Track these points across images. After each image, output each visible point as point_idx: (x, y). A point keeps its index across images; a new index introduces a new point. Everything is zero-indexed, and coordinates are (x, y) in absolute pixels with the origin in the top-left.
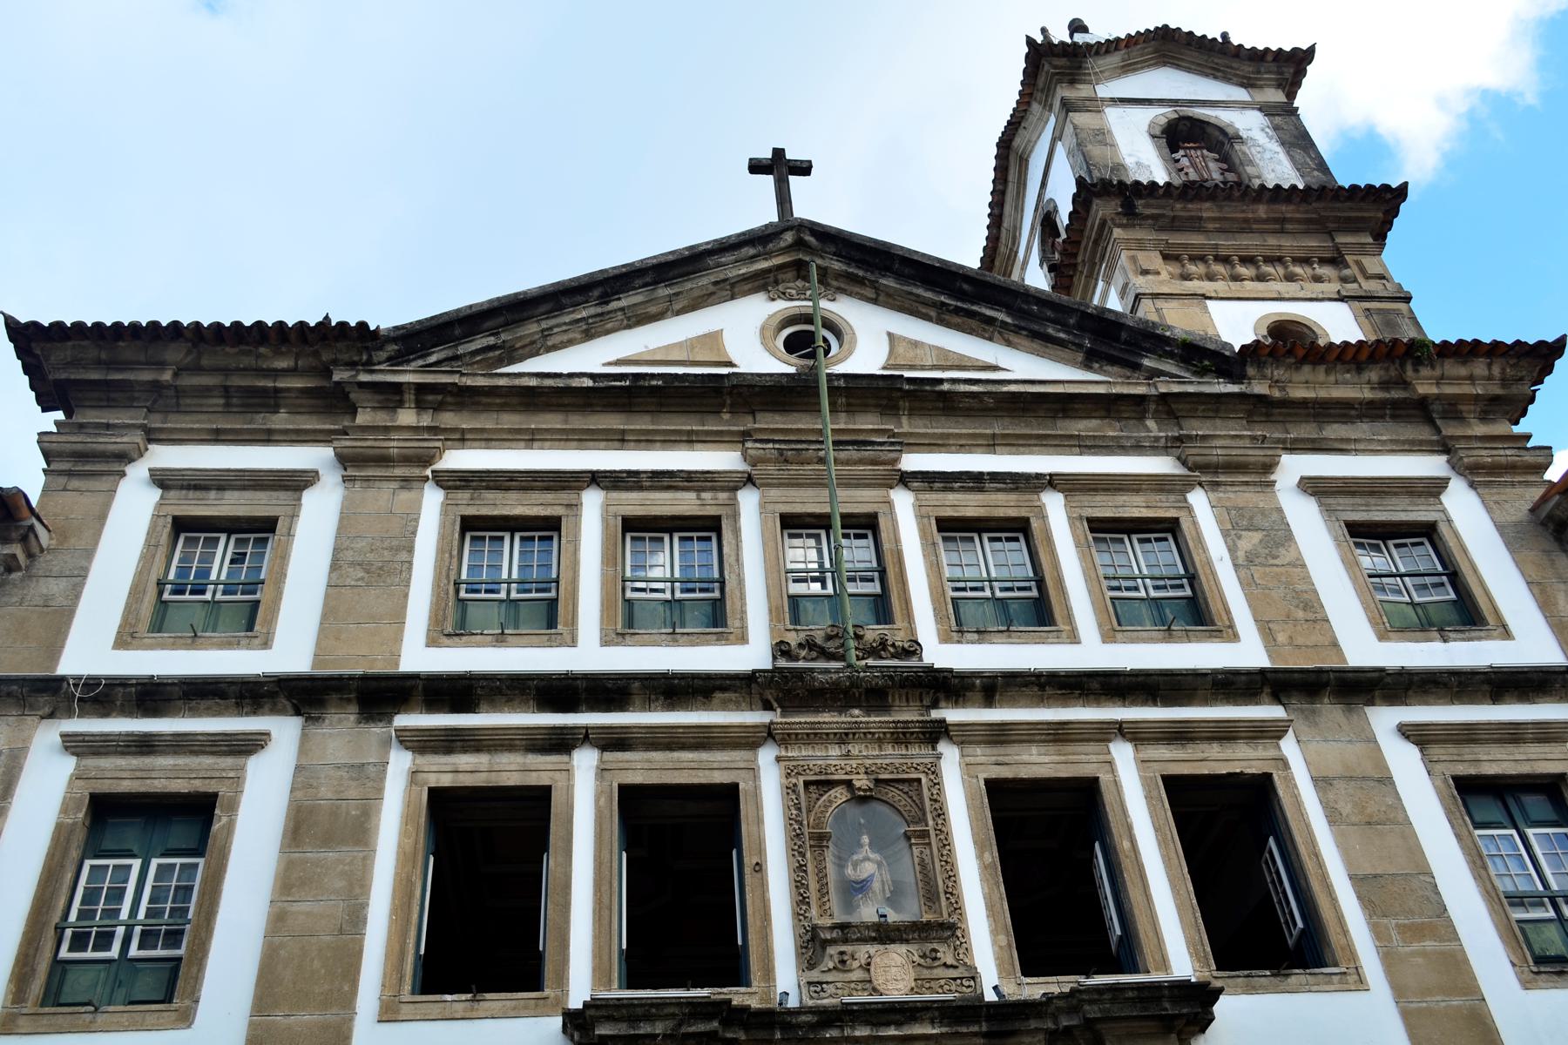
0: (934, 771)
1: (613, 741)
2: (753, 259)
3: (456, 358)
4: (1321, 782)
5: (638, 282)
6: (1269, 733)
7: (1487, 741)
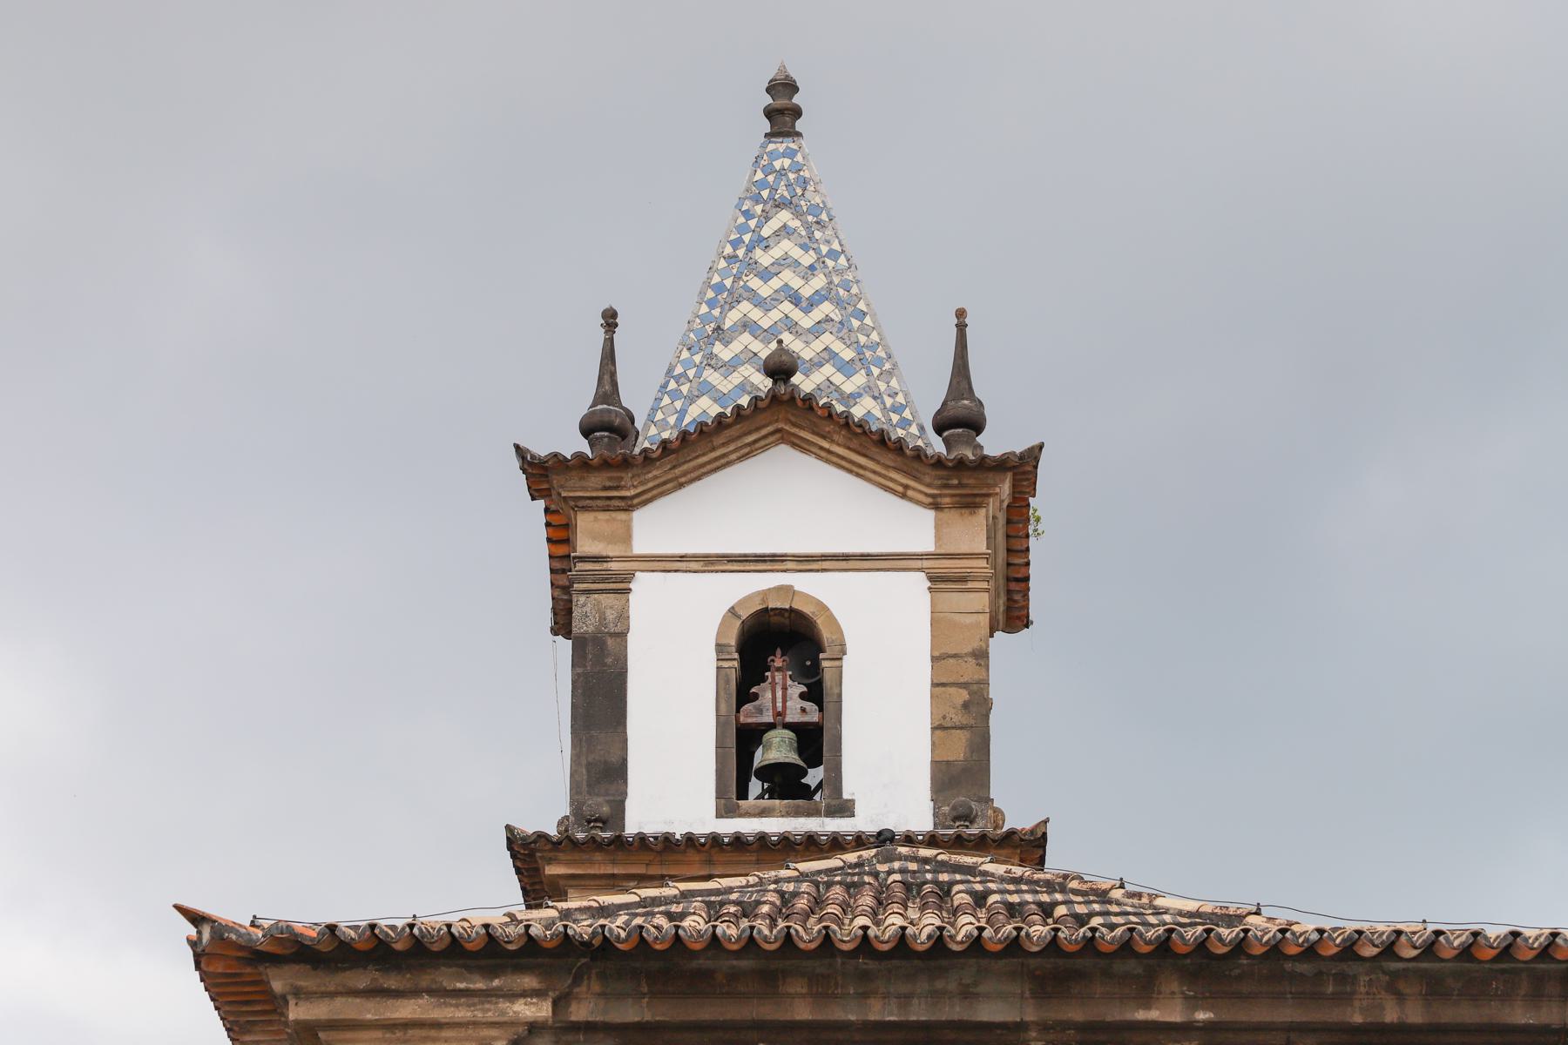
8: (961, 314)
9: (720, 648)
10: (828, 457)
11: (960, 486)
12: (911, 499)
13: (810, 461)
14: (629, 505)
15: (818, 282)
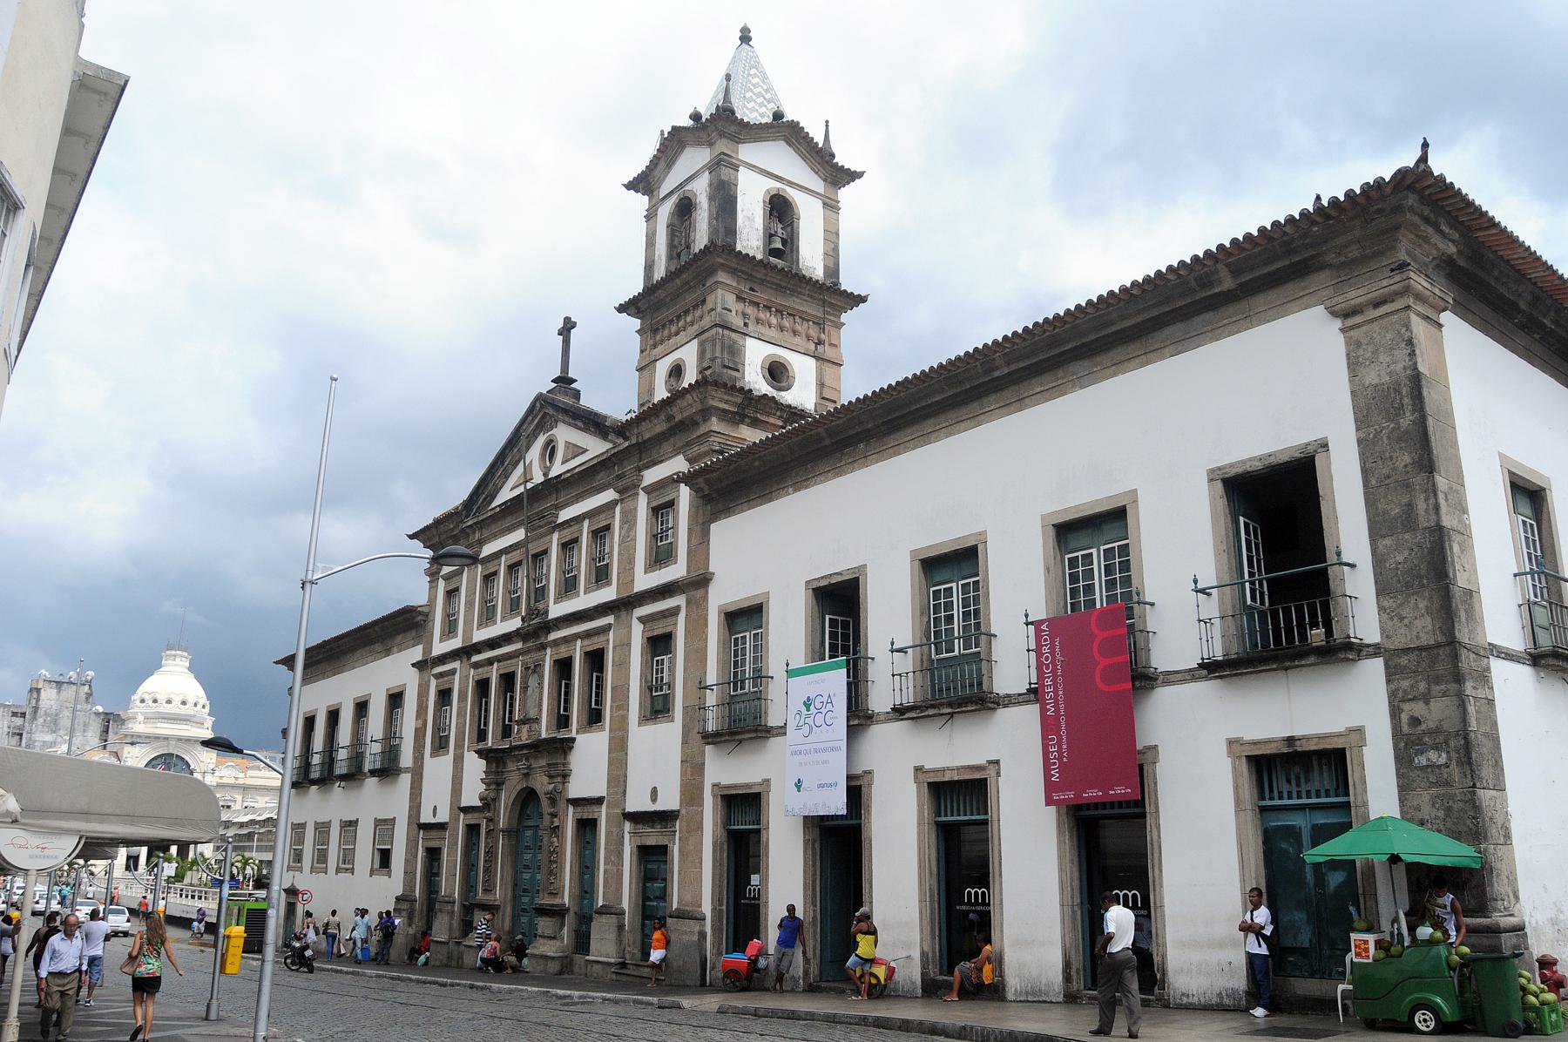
0: (544, 661)
1: (499, 659)
2: (533, 420)
3: (479, 507)
4: (614, 648)
5: (507, 451)
6: (605, 630)
7: (659, 619)
8: (827, 122)
9: (764, 202)
10: (797, 150)
11: (836, 176)
12: (819, 175)
13: (791, 150)
14: (740, 141)
15: (768, 96)
